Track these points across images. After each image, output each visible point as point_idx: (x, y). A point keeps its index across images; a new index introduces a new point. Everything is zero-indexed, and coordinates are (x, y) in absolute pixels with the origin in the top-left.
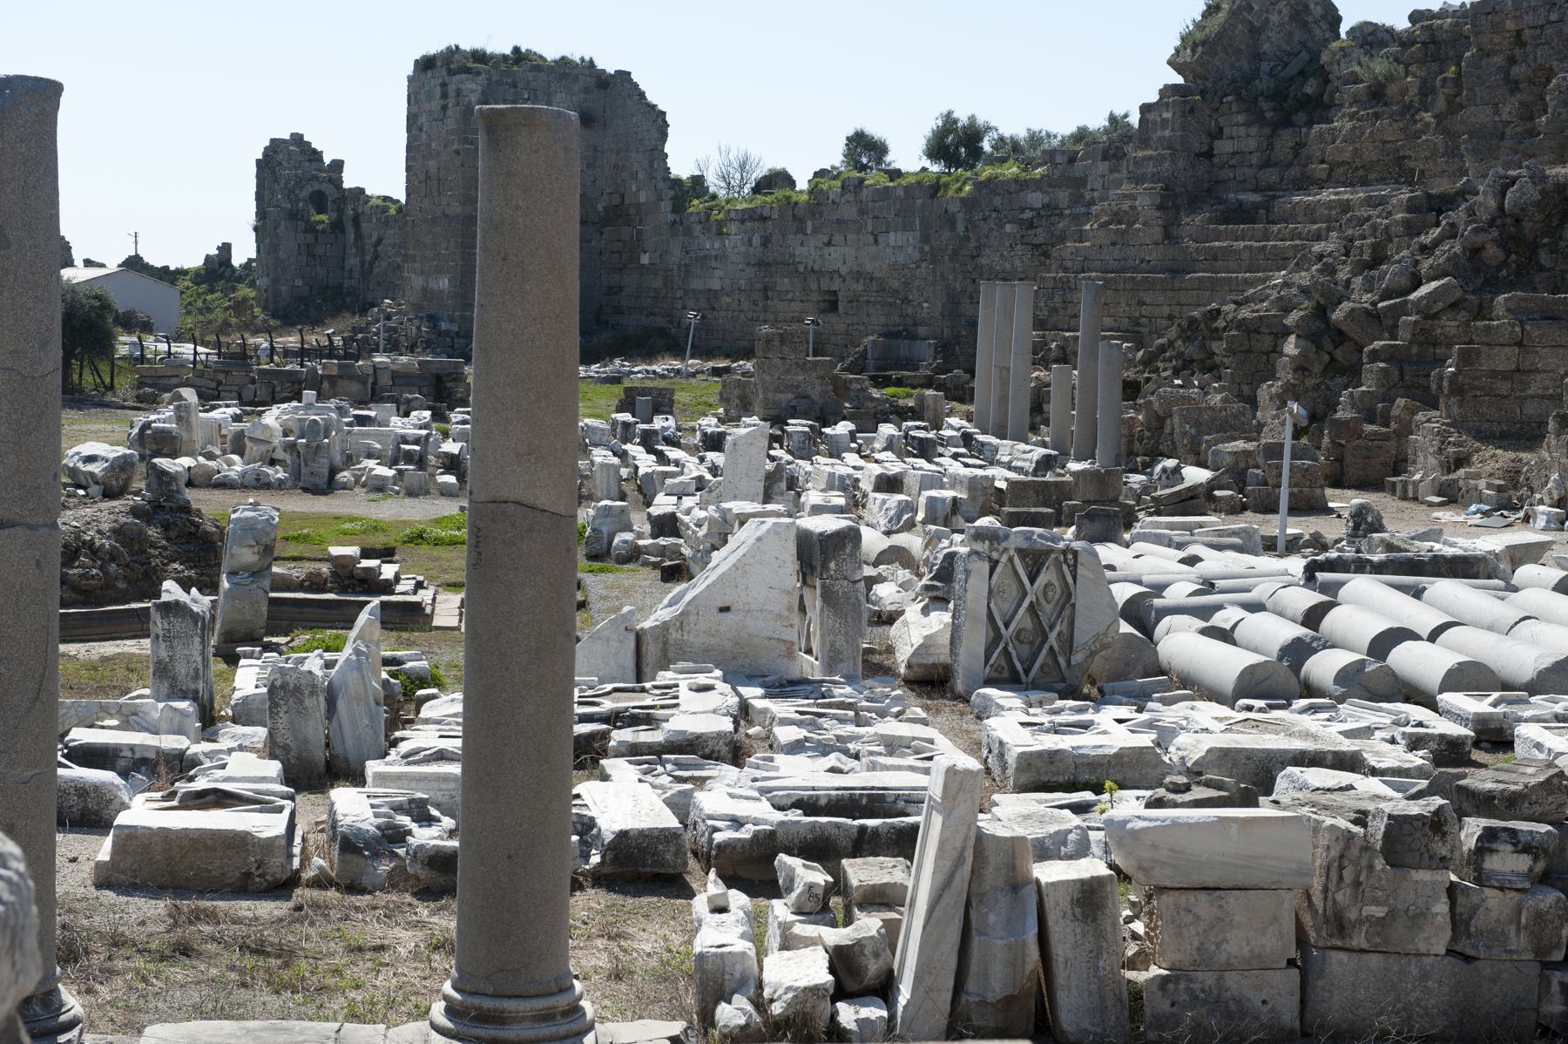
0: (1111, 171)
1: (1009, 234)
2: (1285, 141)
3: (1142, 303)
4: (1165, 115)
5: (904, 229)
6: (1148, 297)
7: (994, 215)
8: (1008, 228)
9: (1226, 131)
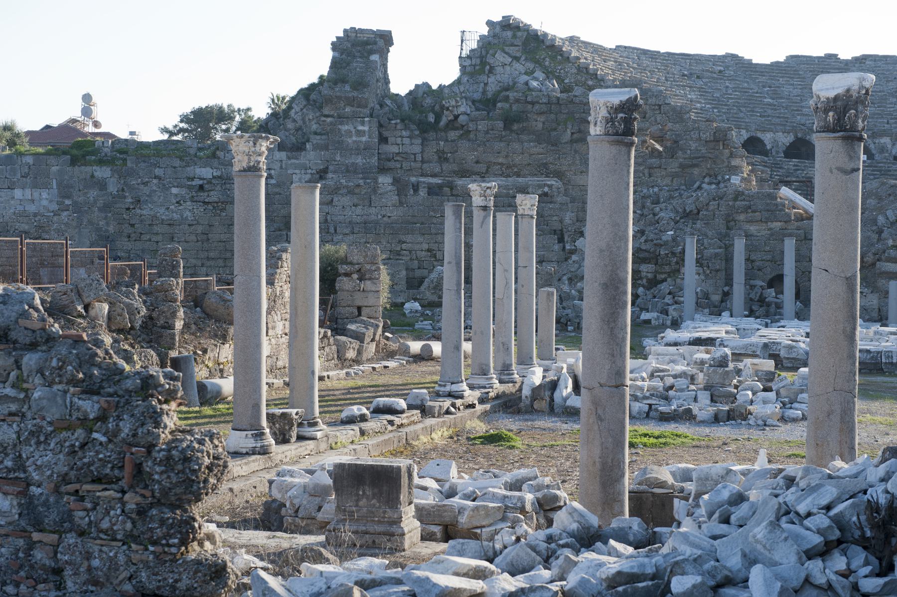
0: (289, 158)
1: (176, 195)
2: (431, 151)
3: (401, 242)
4: (360, 128)
5: (35, 186)
6: (409, 238)
7: (155, 181)
8: (175, 191)
9: (391, 140)
